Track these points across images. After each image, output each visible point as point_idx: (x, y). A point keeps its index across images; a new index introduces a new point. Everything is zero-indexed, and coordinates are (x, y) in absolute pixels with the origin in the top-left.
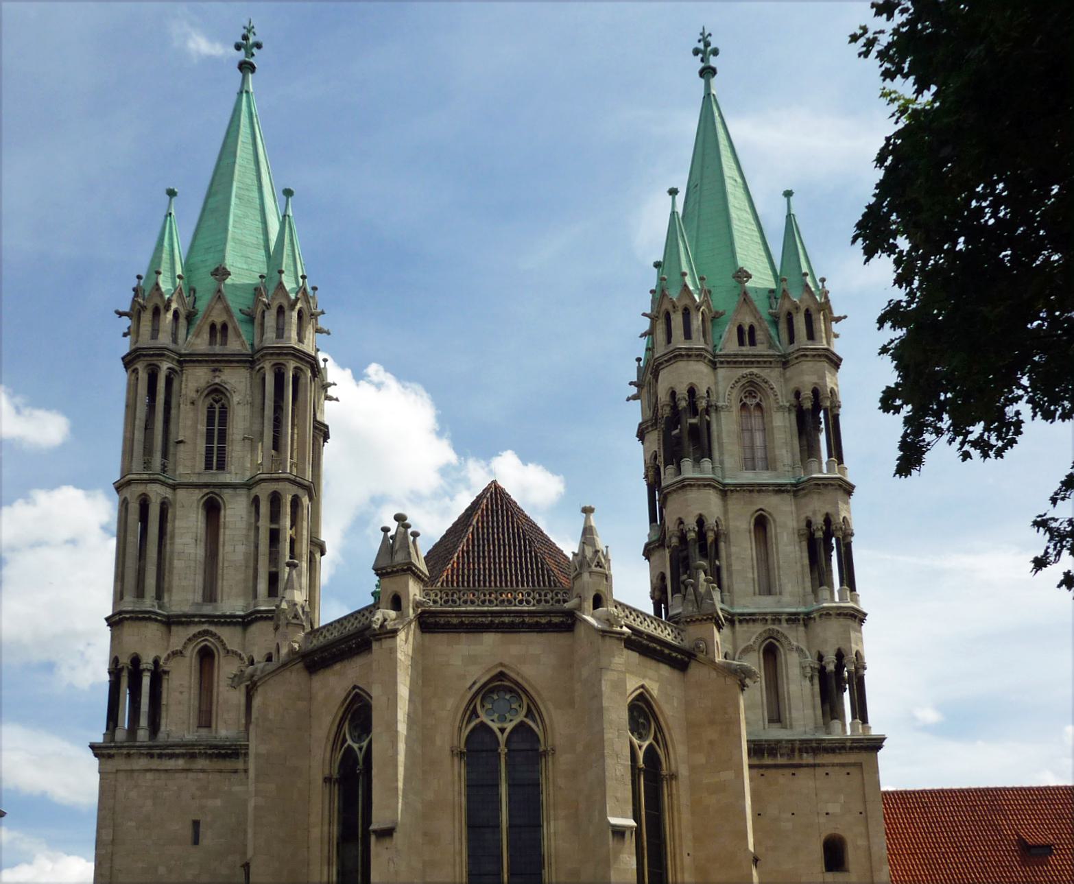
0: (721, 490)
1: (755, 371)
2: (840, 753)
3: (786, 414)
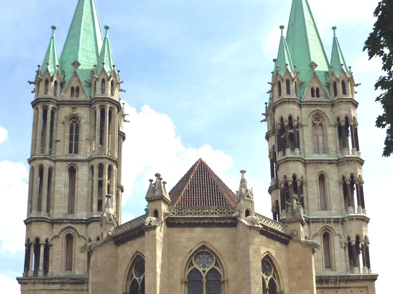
0: (303, 163)
1: (319, 108)
2: (358, 282)
3: (333, 128)
